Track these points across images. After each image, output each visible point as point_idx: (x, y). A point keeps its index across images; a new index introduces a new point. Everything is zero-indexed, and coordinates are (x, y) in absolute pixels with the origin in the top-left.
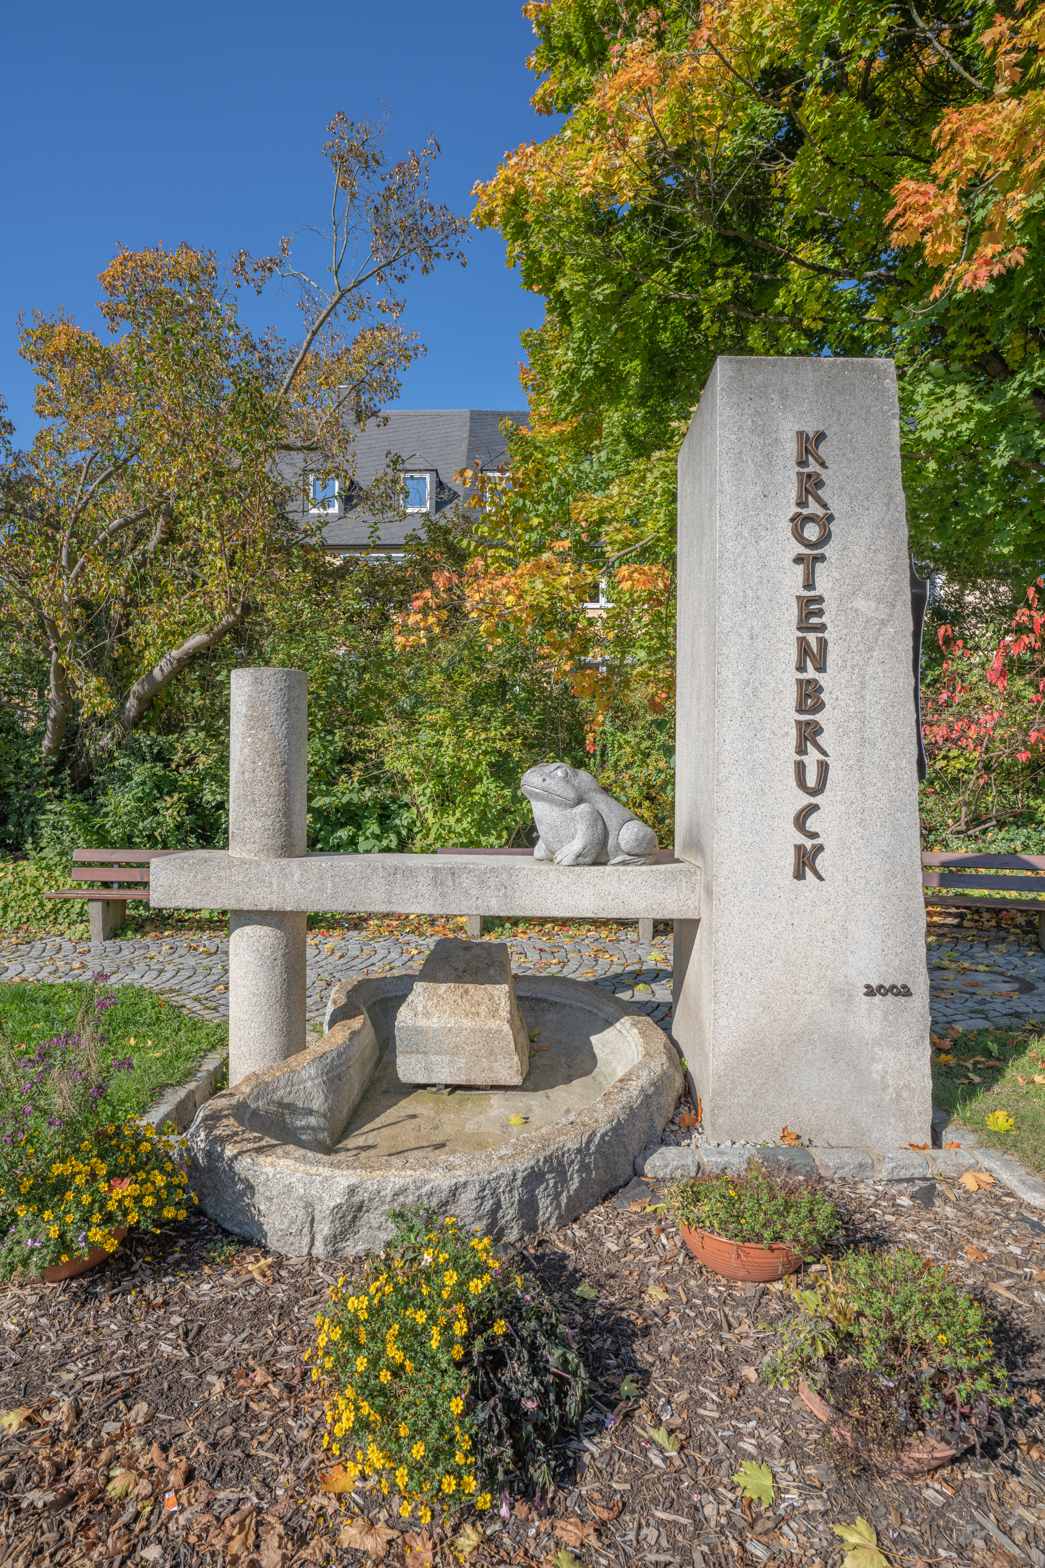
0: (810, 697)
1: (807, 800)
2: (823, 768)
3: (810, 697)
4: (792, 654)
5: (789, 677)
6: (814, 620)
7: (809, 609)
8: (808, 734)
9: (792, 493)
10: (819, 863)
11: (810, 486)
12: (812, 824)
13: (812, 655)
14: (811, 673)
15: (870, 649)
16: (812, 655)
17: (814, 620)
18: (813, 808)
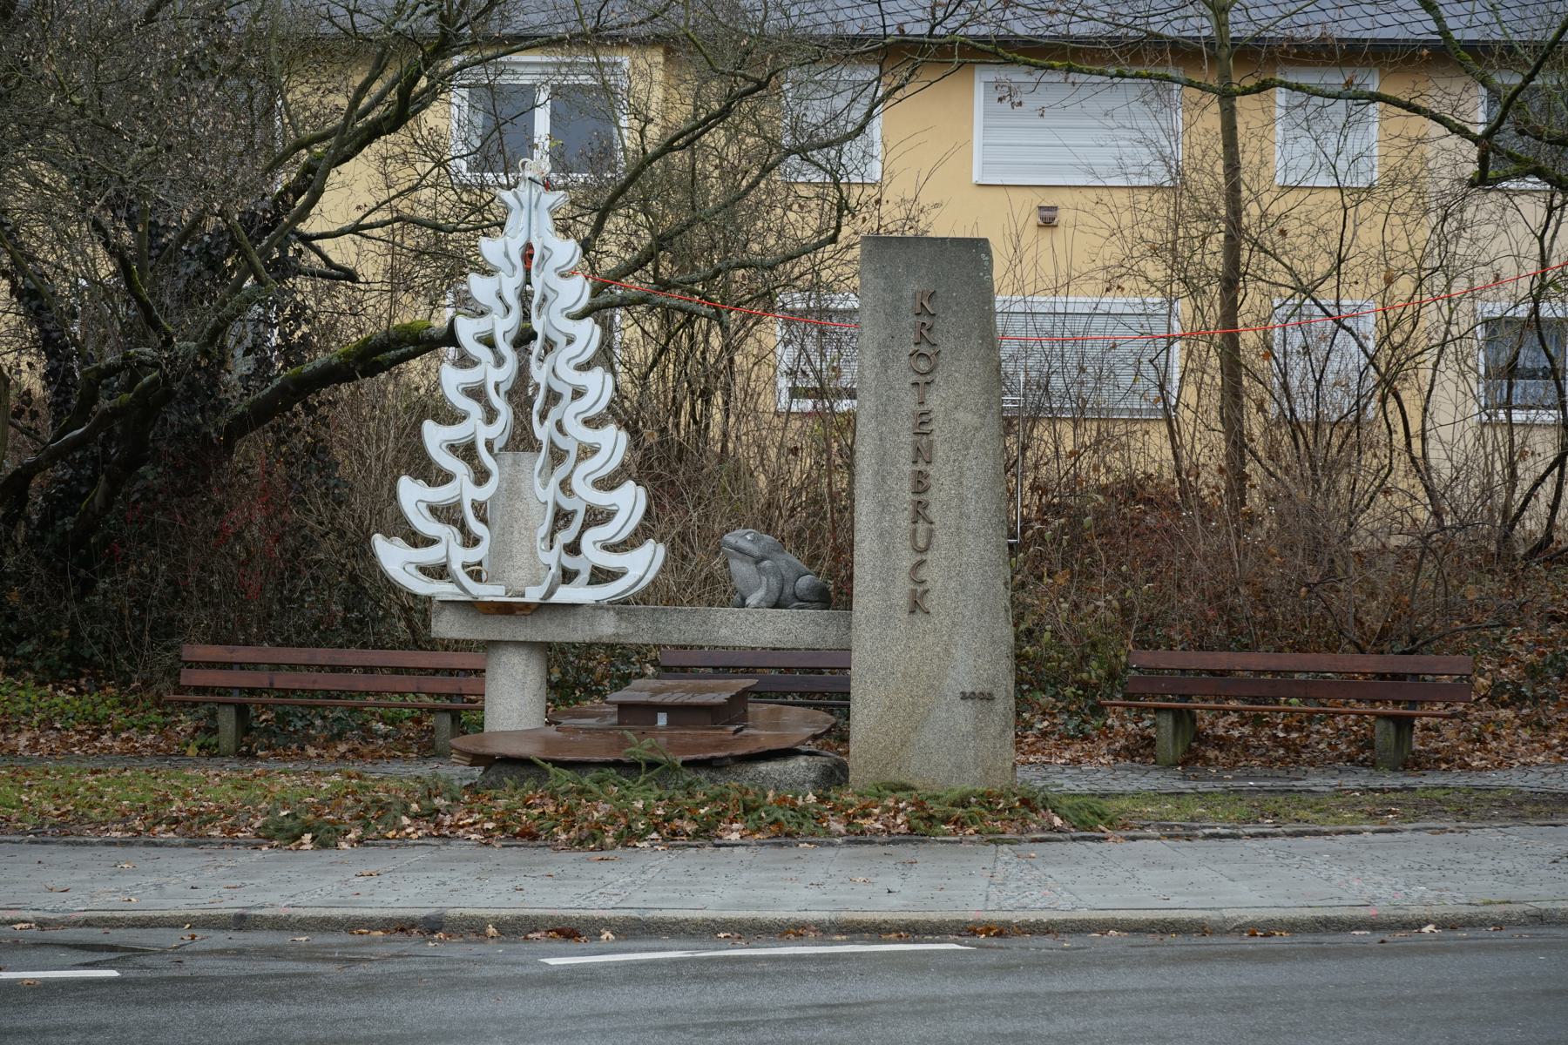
0: (920, 483)
1: (919, 558)
2: (930, 534)
3: (920, 483)
4: (907, 452)
5: (908, 468)
6: (925, 428)
7: (922, 421)
8: (919, 511)
9: (913, 336)
10: (930, 602)
11: (924, 334)
12: (923, 573)
13: (921, 453)
14: (921, 466)
15: (967, 448)
16: (921, 453)
17: (925, 428)
18: (921, 563)
